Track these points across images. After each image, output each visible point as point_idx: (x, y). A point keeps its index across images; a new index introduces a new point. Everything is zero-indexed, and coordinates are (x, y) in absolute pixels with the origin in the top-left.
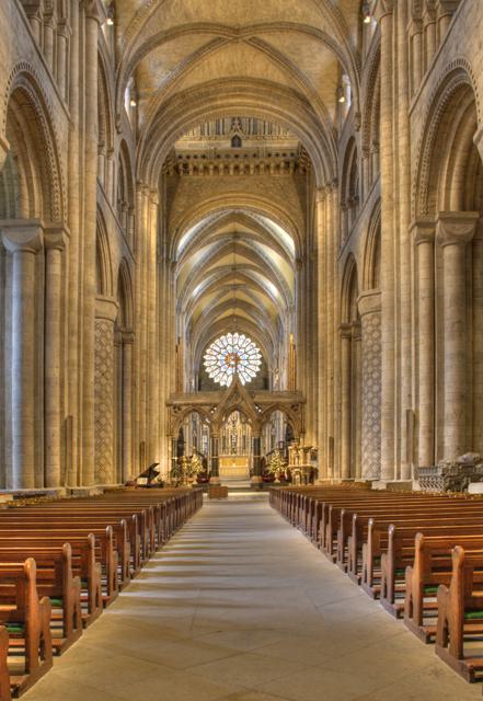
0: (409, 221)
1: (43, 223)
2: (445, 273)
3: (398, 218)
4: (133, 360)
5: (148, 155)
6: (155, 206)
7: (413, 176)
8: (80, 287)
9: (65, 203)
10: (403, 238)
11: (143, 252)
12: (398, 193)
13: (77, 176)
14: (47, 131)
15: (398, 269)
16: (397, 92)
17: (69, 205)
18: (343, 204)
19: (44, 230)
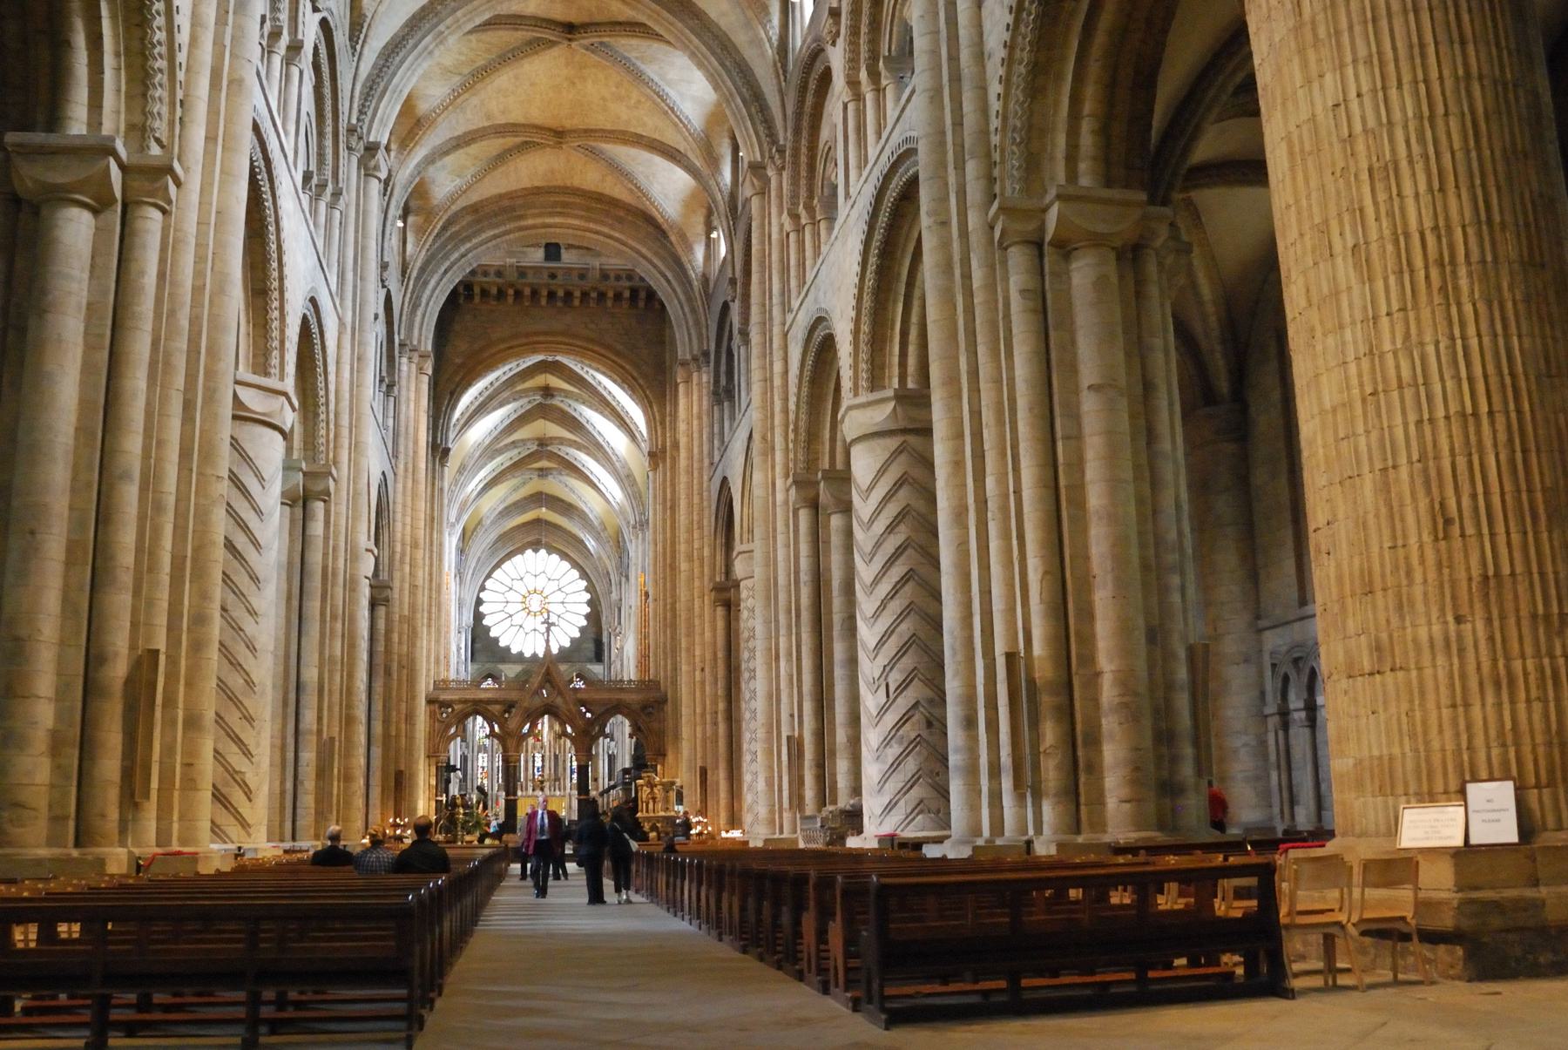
0: (787, 476)
1: (304, 465)
2: (833, 551)
3: (773, 467)
4: (388, 632)
5: (419, 298)
6: (426, 379)
7: (792, 416)
9: (332, 436)
10: (780, 497)
11: (406, 455)
13: (347, 396)
14: (318, 348)
15: (775, 537)
16: (771, 298)
18: (715, 393)
19: (305, 474)
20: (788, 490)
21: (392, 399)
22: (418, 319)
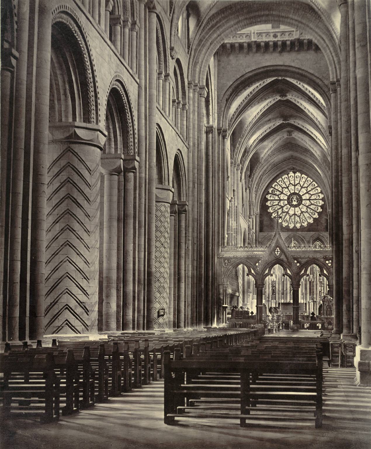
1: (123, 156)
19: (124, 160)
21: (185, 111)
22: (198, 70)
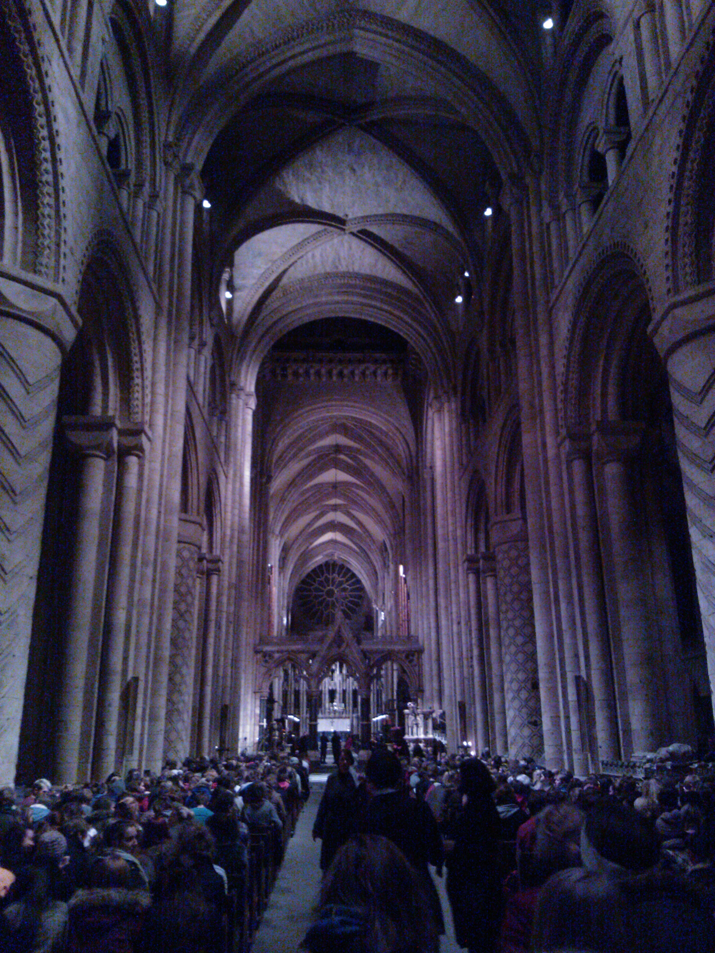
0: (557, 433)
3: (543, 429)
8: (160, 504)
10: (551, 452)
12: (541, 401)
16: (533, 284)
17: (153, 403)
20: (559, 446)
